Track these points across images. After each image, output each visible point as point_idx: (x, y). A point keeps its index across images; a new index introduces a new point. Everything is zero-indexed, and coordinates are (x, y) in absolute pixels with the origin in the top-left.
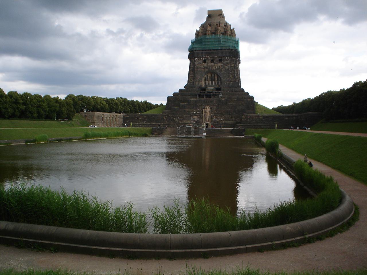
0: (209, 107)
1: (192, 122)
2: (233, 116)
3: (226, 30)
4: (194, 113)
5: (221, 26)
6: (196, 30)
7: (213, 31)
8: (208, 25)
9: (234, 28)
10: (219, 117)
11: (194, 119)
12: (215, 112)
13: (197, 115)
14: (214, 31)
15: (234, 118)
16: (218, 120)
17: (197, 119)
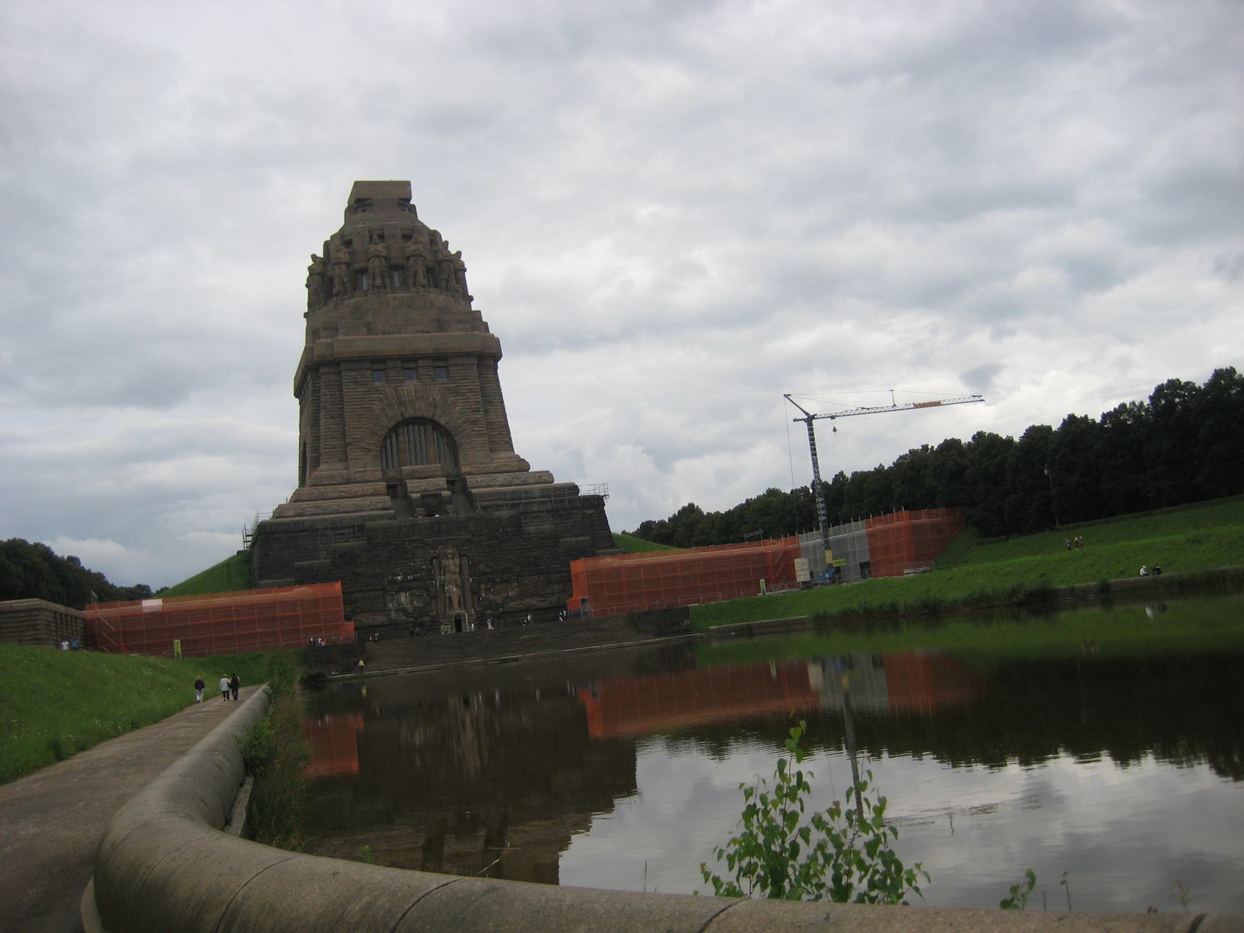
1: (393, 615)
2: (554, 576)
3: (440, 257)
4: (396, 582)
6: (314, 257)
7: (394, 261)
8: (375, 237)
9: (459, 254)
10: (498, 587)
11: (400, 604)
12: (482, 567)
13: (409, 589)
14: (401, 261)
15: (558, 583)
16: (498, 599)
17: (412, 603)
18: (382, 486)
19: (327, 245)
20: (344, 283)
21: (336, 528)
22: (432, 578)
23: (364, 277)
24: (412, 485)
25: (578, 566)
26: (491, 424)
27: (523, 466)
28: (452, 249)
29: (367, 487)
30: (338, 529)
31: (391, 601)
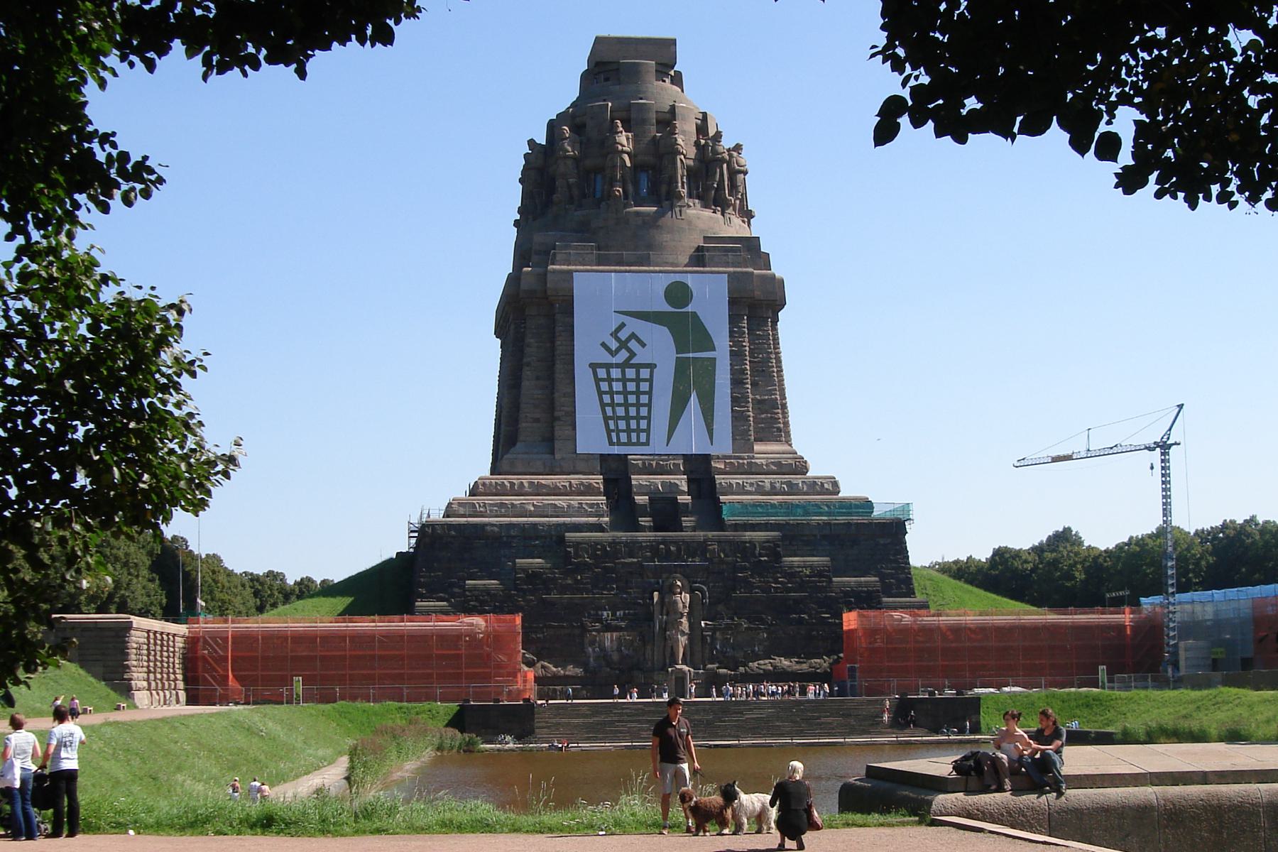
0: (686, 583)
5: (684, 133)
6: (531, 143)
9: (738, 148)
18: (597, 480)
19: (552, 126)
20: (569, 186)
21: (529, 539)
22: (650, 618)
23: (599, 177)
24: (637, 480)
25: (850, 620)
26: (760, 402)
27: (800, 467)
28: (727, 143)
29: (575, 479)
30: (531, 538)
31: (592, 643)
